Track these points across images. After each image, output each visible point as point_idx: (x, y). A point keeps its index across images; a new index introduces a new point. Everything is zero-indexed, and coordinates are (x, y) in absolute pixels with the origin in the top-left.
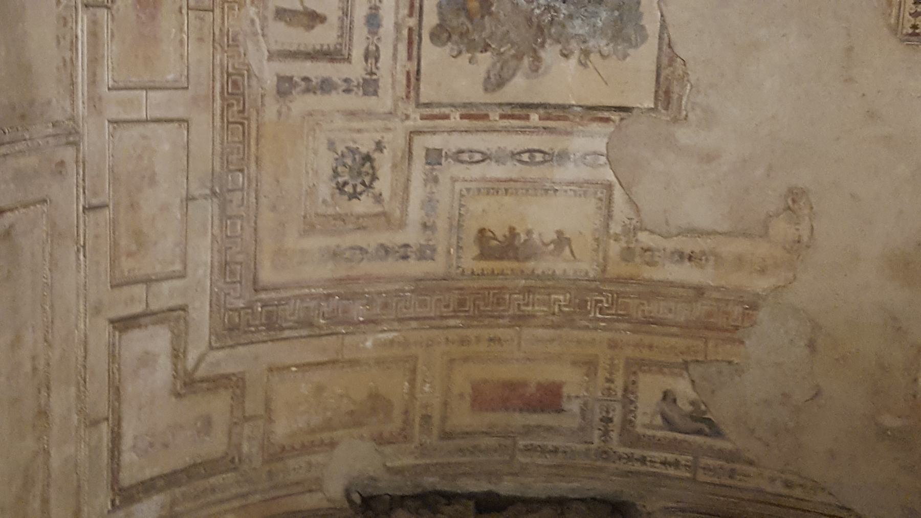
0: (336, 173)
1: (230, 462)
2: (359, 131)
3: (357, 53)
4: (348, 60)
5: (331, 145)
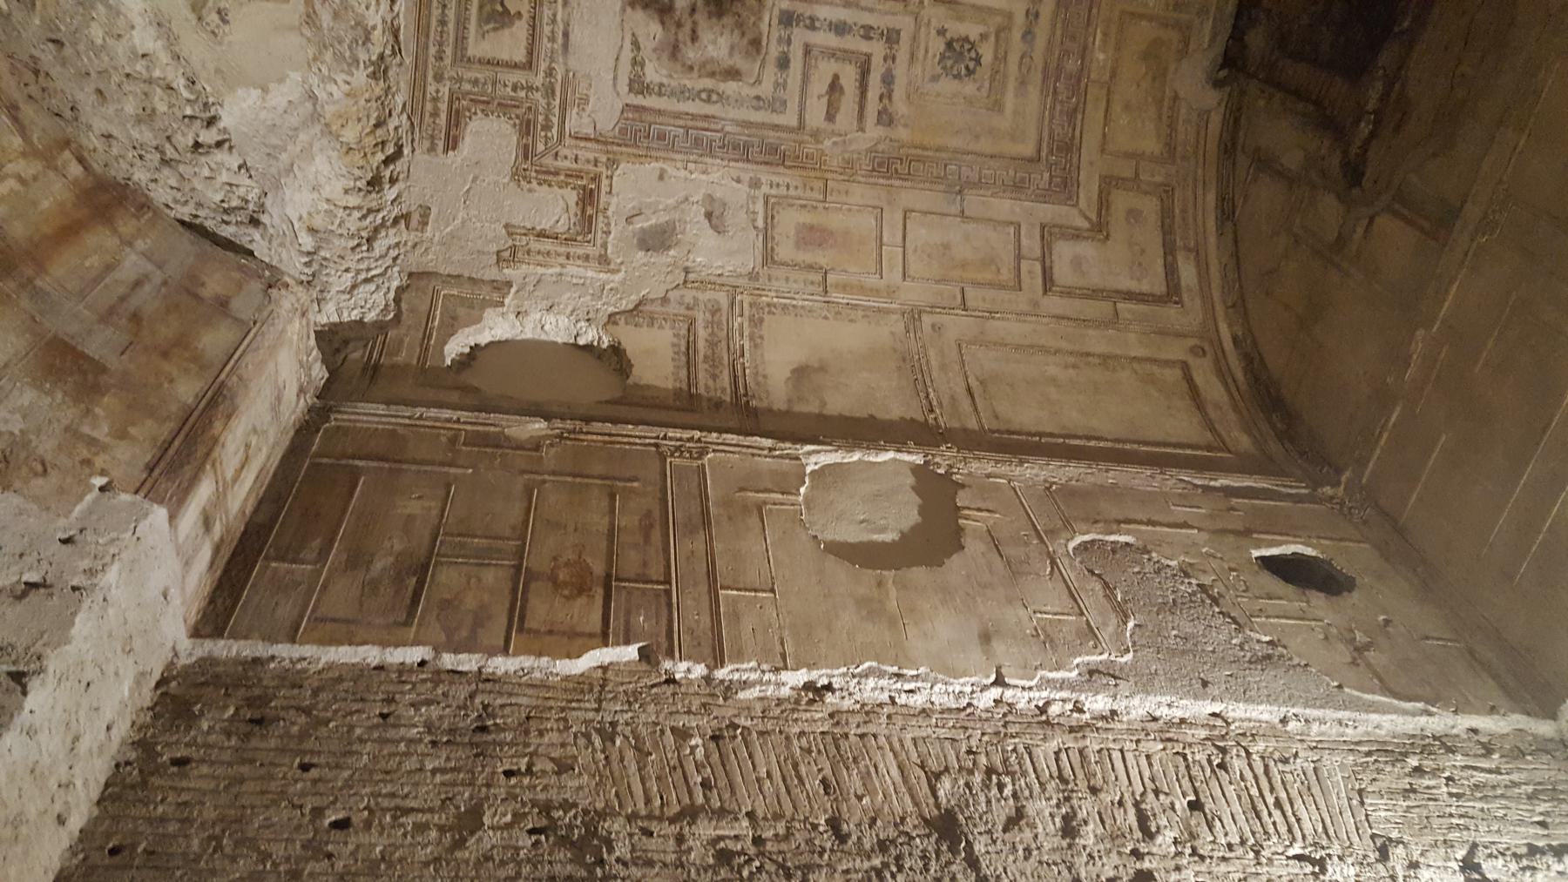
0: (958, 77)
1: (1166, 193)
2: (927, 51)
3: (865, 47)
4: (869, 56)
5: (935, 78)
